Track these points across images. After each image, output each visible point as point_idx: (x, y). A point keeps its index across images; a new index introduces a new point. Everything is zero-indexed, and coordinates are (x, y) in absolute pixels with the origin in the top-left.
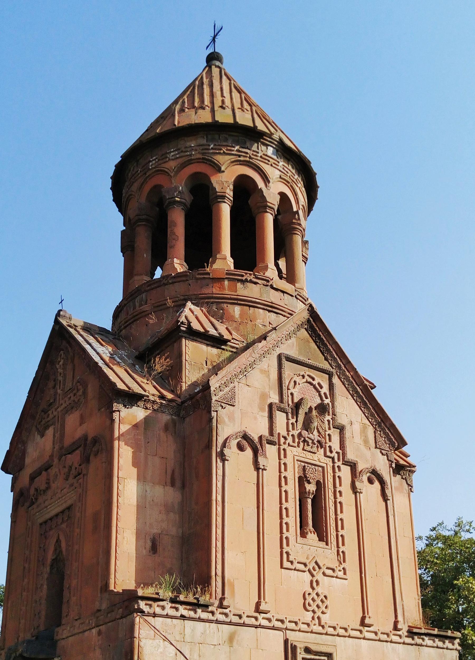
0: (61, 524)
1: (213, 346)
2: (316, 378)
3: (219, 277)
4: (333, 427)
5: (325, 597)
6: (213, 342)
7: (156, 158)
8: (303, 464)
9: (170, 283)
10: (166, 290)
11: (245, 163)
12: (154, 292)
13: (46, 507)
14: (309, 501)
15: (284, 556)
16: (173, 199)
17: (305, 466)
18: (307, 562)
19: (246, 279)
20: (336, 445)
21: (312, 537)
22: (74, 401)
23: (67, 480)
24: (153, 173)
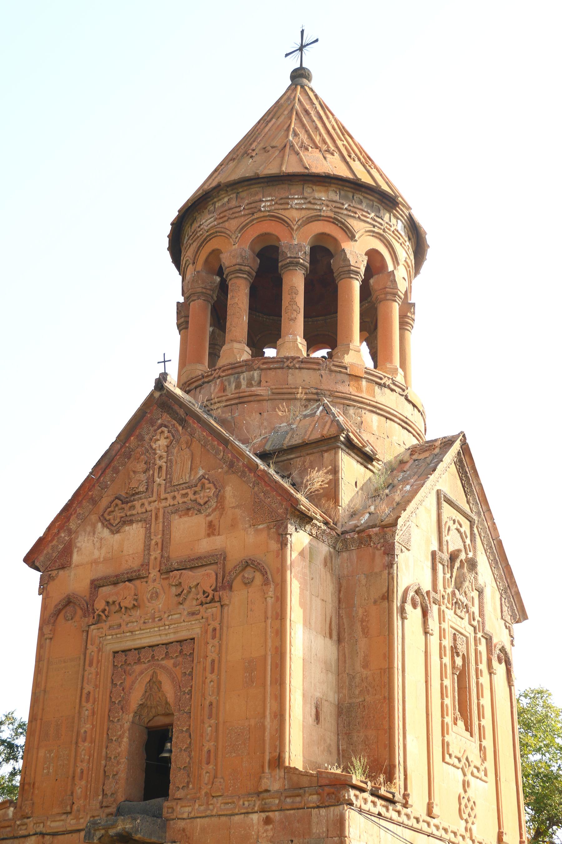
0: (162, 659)
1: (361, 464)
2: (463, 526)
3: (357, 375)
4: (476, 589)
5: (474, 803)
6: (362, 458)
7: (272, 200)
8: (454, 631)
9: (297, 368)
10: (290, 375)
11: (378, 236)
12: (272, 373)
13: (132, 632)
14: (456, 677)
15: (445, 745)
16: (297, 259)
17: (455, 634)
18: (459, 755)
19: (384, 383)
20: (475, 609)
21: (461, 723)
22: (196, 500)
23: (181, 604)
24: (264, 216)
